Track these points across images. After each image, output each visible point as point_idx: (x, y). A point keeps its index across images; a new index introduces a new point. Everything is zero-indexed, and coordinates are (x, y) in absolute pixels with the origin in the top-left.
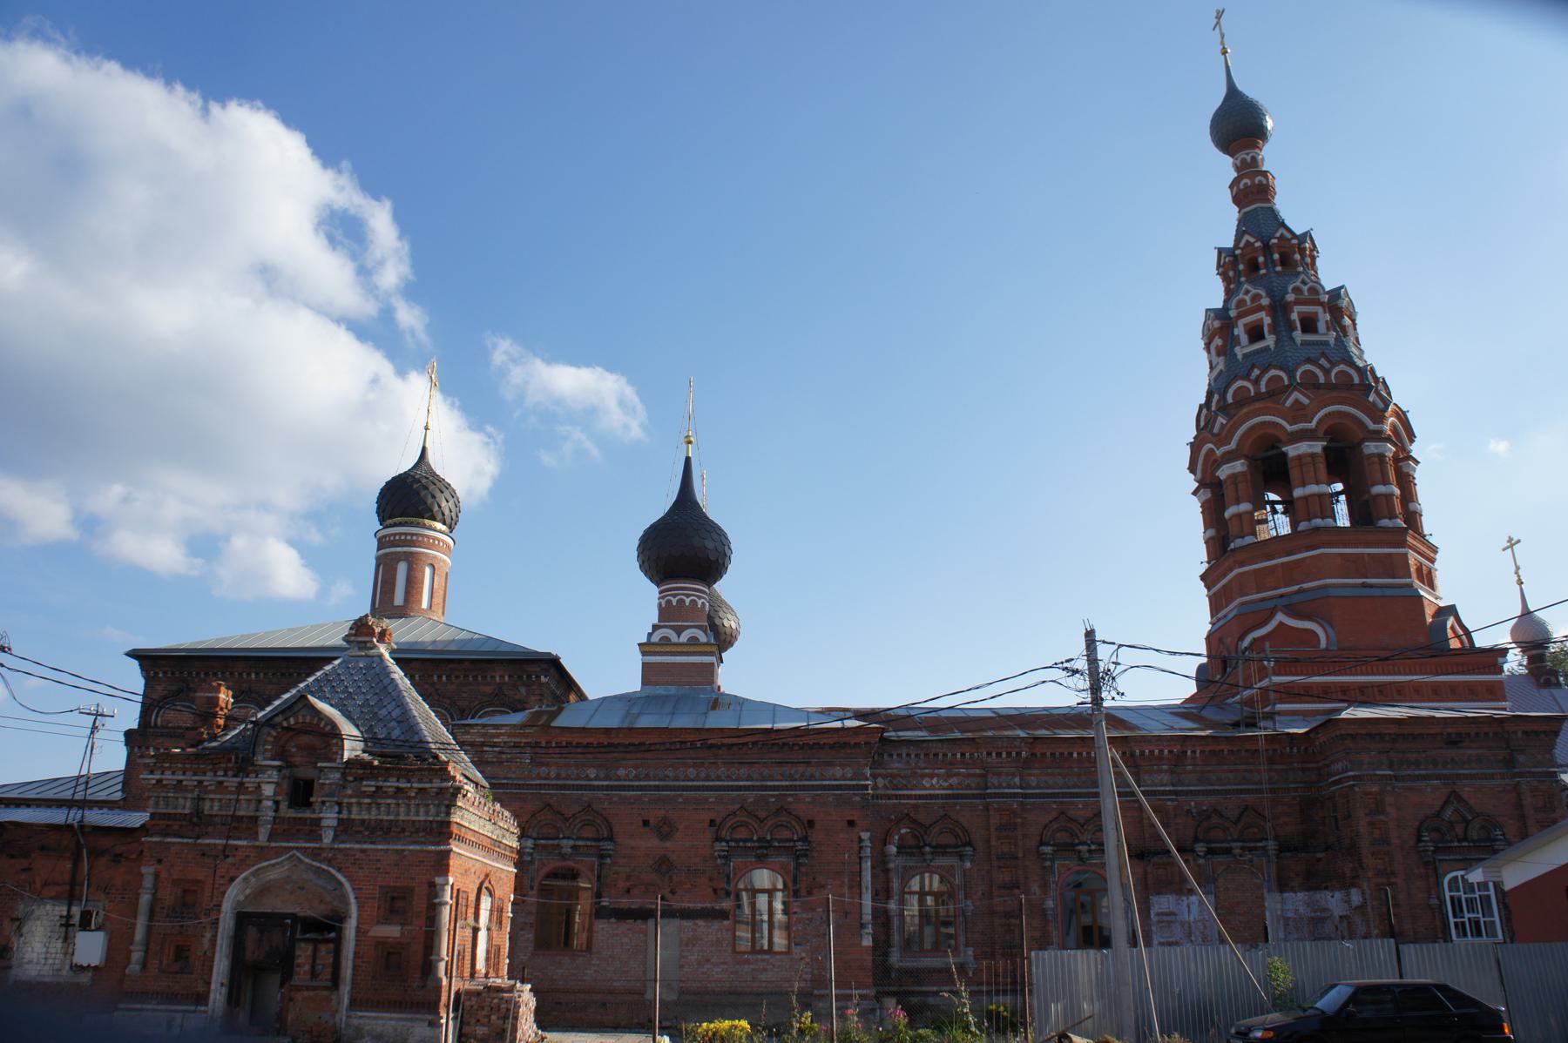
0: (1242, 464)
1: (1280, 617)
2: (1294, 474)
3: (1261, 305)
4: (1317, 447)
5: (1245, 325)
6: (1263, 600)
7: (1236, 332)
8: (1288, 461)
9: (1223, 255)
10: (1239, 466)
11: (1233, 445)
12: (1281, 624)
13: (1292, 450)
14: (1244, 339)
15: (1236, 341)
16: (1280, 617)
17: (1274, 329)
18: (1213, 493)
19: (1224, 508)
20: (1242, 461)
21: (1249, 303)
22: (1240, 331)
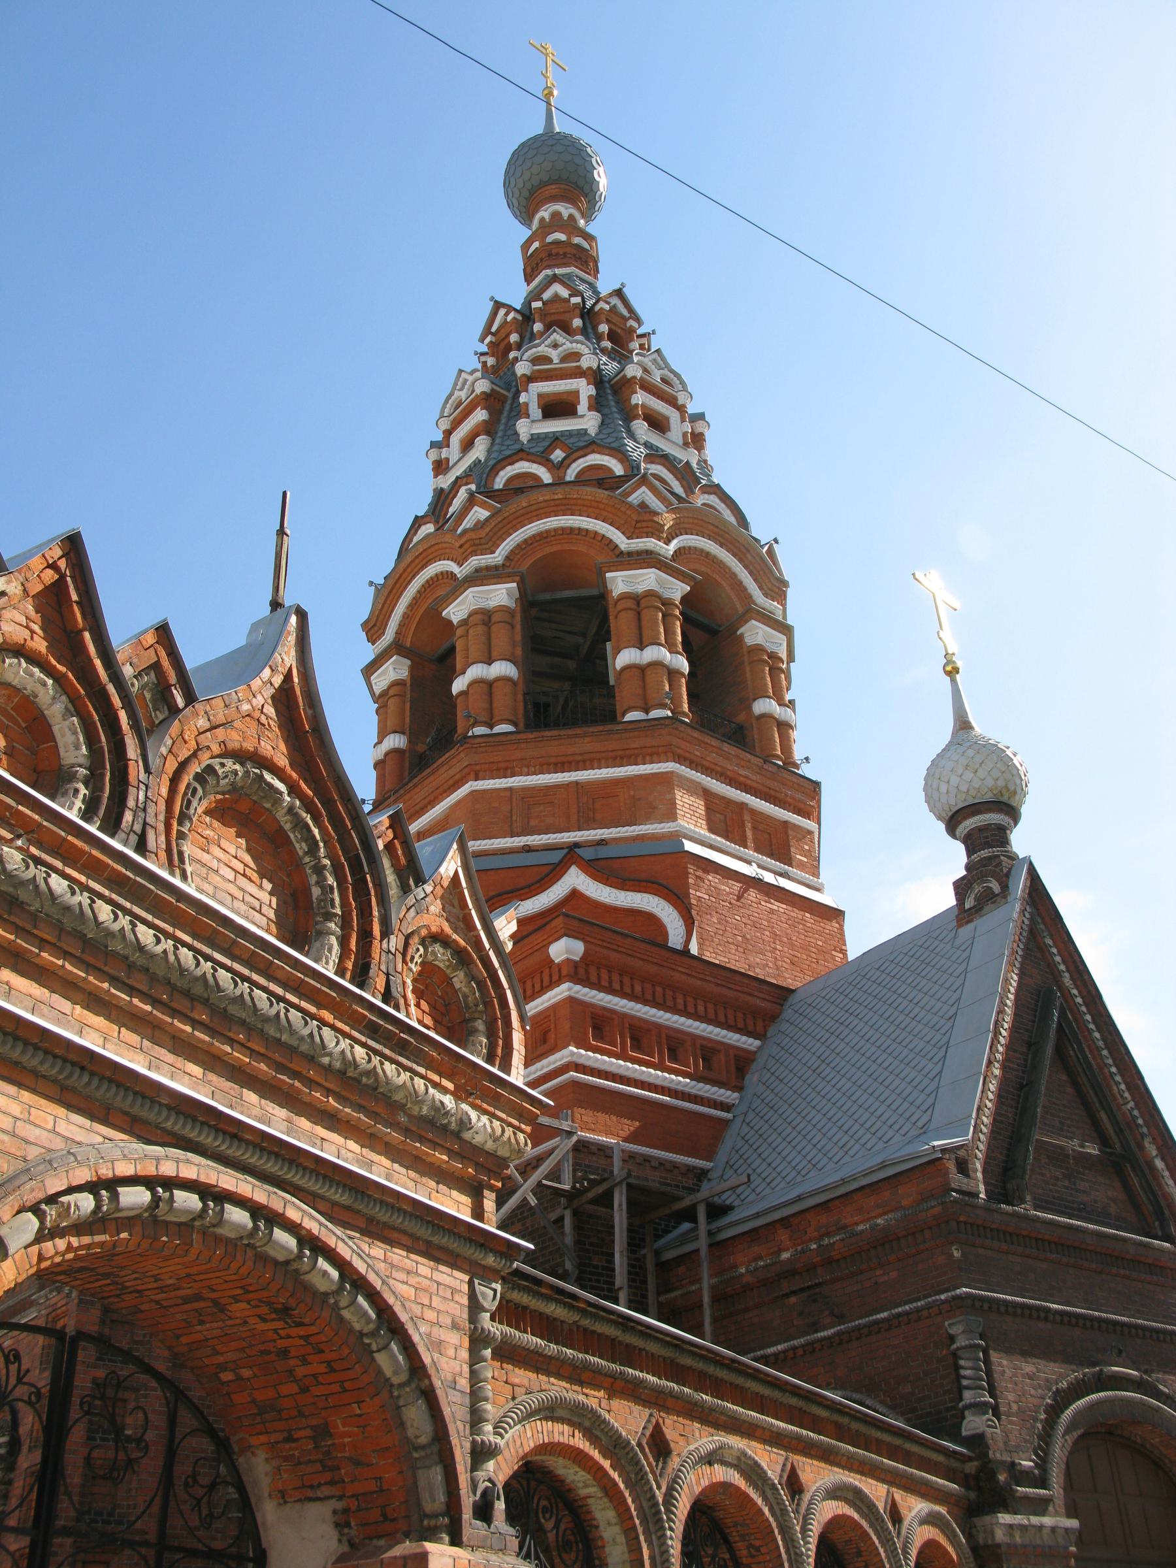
0: (509, 594)
1: (575, 879)
2: (621, 623)
3: (579, 367)
4: (677, 590)
5: (540, 396)
6: (528, 849)
7: (523, 398)
8: (611, 603)
9: (502, 312)
10: (501, 595)
11: (497, 557)
12: (575, 894)
13: (620, 582)
14: (535, 411)
15: (521, 412)
16: (575, 879)
17: (597, 404)
18: (412, 669)
19: (451, 674)
20: (514, 585)
21: (556, 360)
22: (530, 397)
